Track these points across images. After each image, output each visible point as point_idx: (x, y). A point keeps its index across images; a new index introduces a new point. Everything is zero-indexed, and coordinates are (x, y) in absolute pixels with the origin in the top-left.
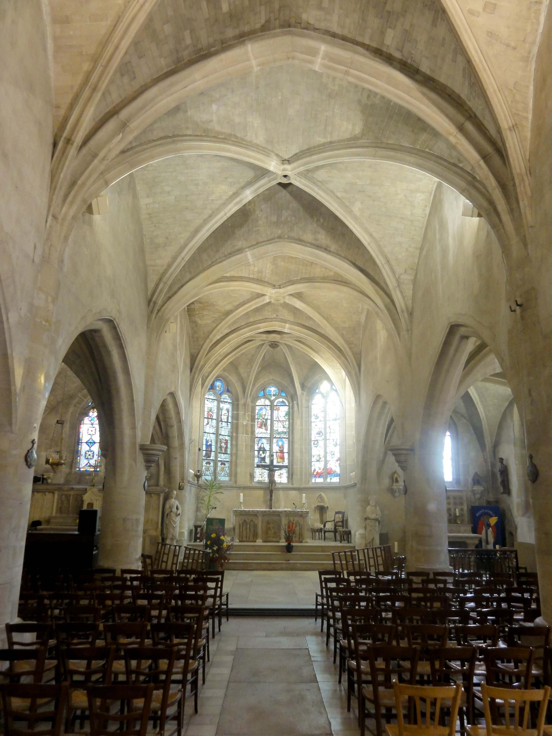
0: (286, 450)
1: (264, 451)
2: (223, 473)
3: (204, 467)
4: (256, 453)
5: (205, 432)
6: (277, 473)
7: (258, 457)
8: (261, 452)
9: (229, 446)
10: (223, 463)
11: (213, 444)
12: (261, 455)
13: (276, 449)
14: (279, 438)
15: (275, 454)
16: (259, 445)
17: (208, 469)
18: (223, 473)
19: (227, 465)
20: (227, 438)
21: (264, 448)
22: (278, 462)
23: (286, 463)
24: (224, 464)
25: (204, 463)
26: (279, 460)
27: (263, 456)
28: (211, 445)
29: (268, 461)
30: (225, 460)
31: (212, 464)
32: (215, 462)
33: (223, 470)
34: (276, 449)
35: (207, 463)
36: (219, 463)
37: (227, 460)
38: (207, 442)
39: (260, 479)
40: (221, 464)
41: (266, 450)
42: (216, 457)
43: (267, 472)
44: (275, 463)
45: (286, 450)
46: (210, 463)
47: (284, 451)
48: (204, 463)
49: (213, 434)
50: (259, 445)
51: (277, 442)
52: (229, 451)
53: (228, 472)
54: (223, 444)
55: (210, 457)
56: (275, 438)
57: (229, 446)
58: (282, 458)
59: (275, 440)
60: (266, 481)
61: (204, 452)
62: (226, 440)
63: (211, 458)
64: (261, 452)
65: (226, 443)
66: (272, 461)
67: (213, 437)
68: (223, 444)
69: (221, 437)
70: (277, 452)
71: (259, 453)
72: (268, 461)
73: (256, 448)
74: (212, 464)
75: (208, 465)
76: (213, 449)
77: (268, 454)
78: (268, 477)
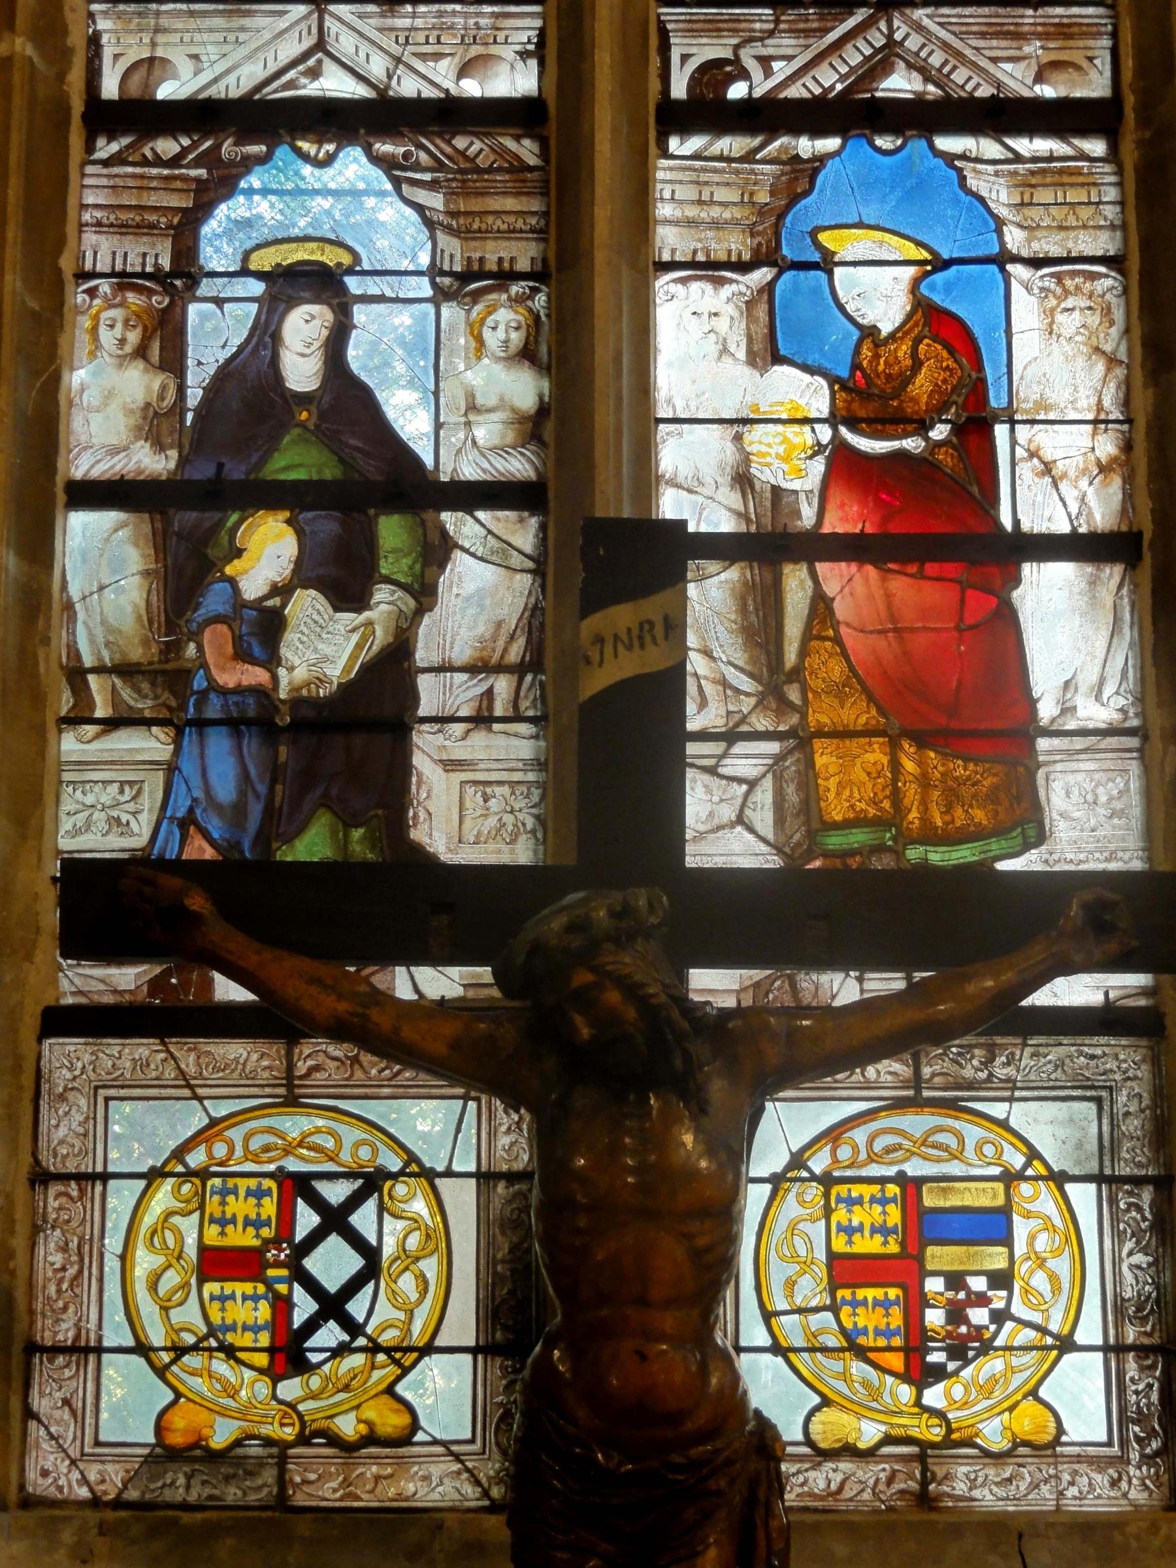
0: (1059, 463)
1: (370, 501)
4: (102, 565)
6: (801, 1180)
7: (164, 686)
8: (267, 551)
12: (265, 628)
13: (724, 409)
14: (855, 113)
15: (711, 597)
16: (215, 333)
21: (347, 401)
22: (803, 810)
23: (1086, 820)
26: (852, 778)
27: (323, 649)
29: (471, 800)
34: (724, 409)
39: (236, 1401)
41: (415, 490)
43: (433, 1123)
44: (726, 822)
45: (1059, 463)
47: (1032, 502)
50: (215, 333)
51: (776, 254)
56: (707, 111)
58: (972, 709)
59: (692, 189)
60: (434, 1485)
64: (267, 551)
66: (612, 749)
70: (768, 545)
71: (187, 571)
72: (471, 800)
73: (107, 408)
77: (482, 587)
78: (507, 1332)
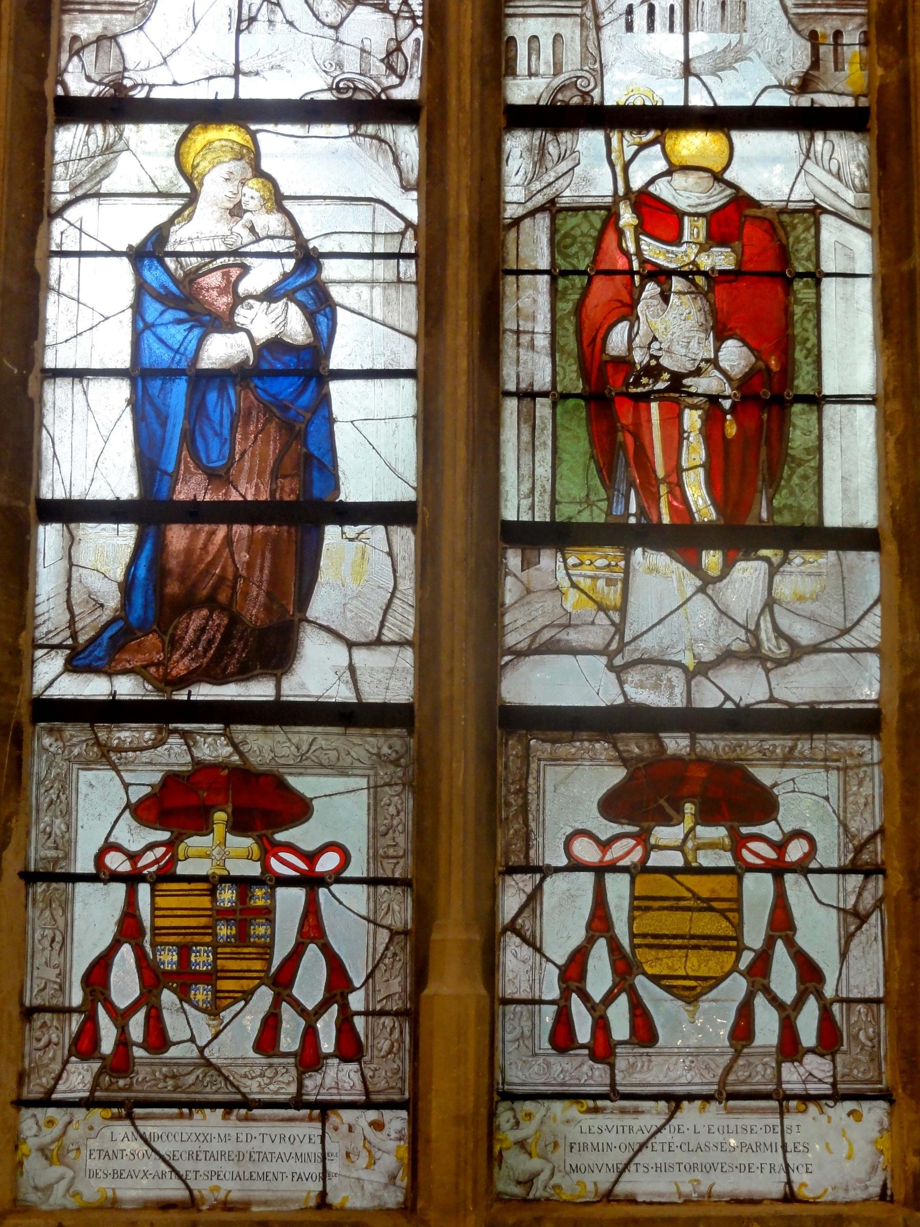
2: (693, 1033)
3: (95, 913)
5: (117, 107)
9: (848, 344)
10: (690, 770)
11: (373, 326)
17: (209, 947)
18: (693, 1033)
19: (811, 800)
20: (769, 168)
24: (738, 800)
25: (96, 808)
28: (297, 378)
30: (746, 687)
31: (341, 811)
32: (461, 751)
33: (675, 934)
35: (174, 806)
36: (573, 795)
37: (803, 685)
38: (171, 286)
40: (638, 802)
42: (460, 618)
46: (265, 805)
48: (96, 808)
49: (358, 109)
52: (850, 472)
53: (864, 972)
54: (671, 331)
55: (275, 649)
57: (848, 344)
61: (109, 549)
62: (736, 216)
63: (317, 672)
65: (763, 268)
67: (354, 191)
68: (671, 331)
69: (590, 167)
74: (341, 811)
75: (220, 850)
76: (374, 439)
